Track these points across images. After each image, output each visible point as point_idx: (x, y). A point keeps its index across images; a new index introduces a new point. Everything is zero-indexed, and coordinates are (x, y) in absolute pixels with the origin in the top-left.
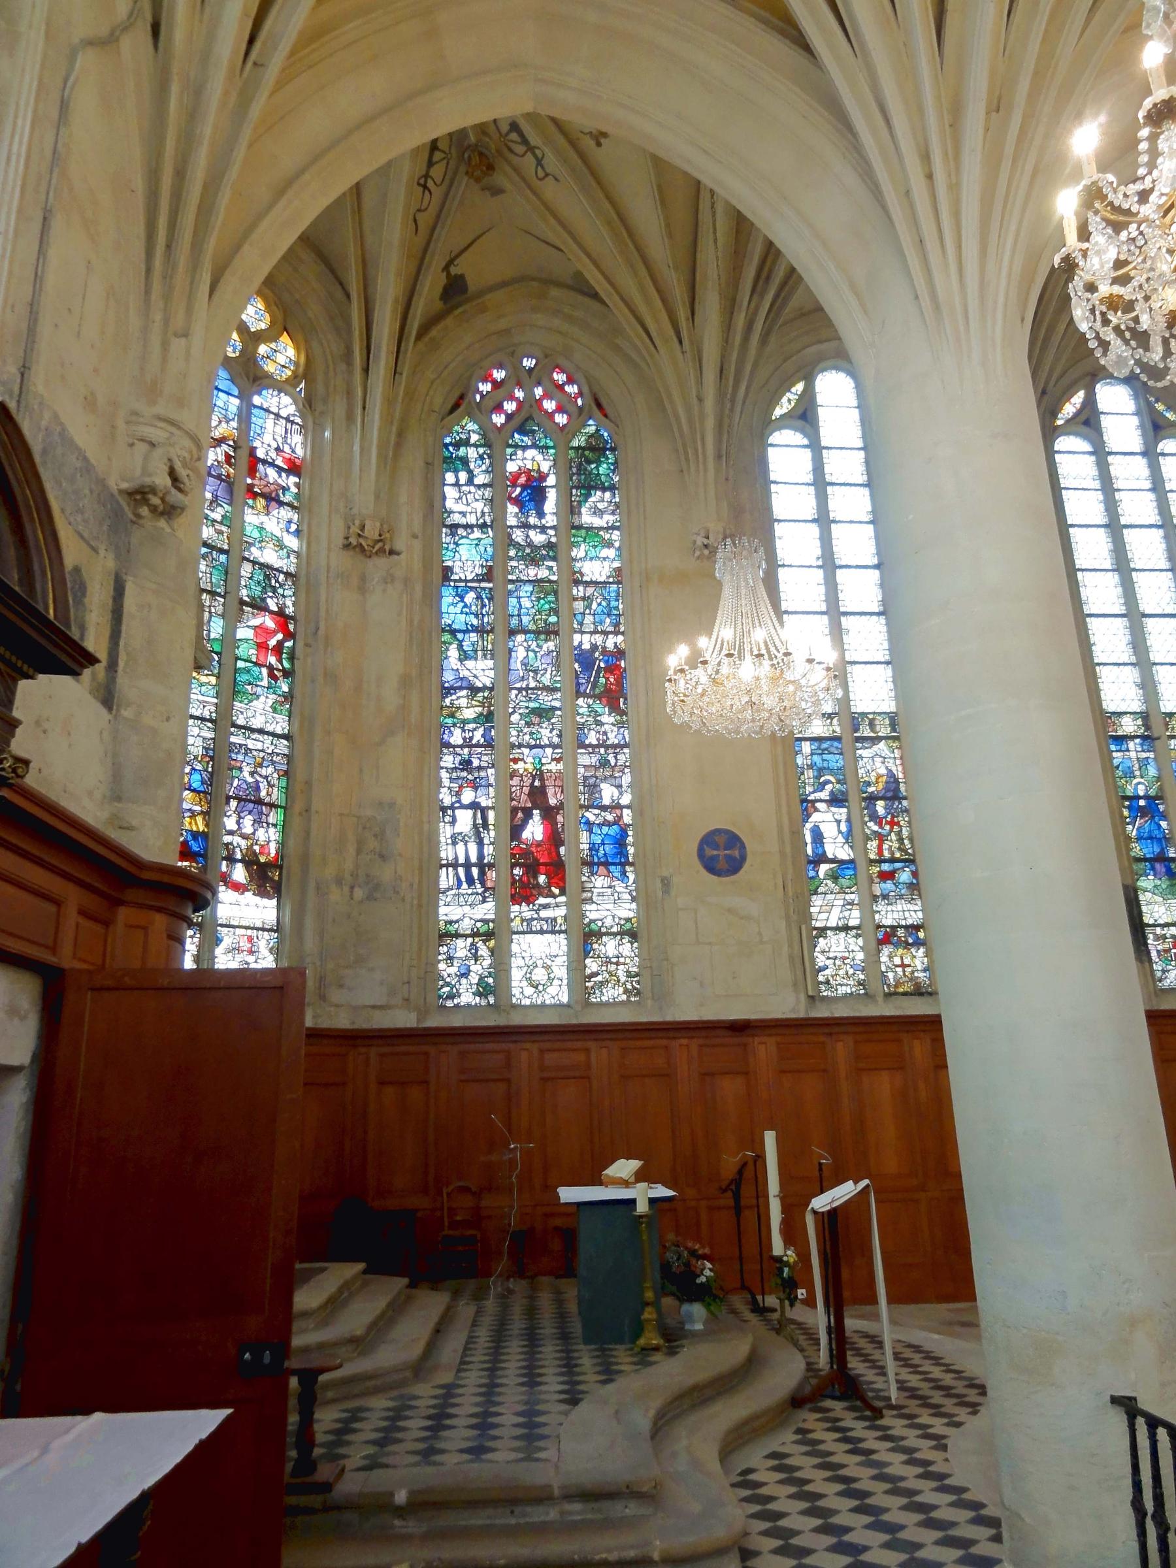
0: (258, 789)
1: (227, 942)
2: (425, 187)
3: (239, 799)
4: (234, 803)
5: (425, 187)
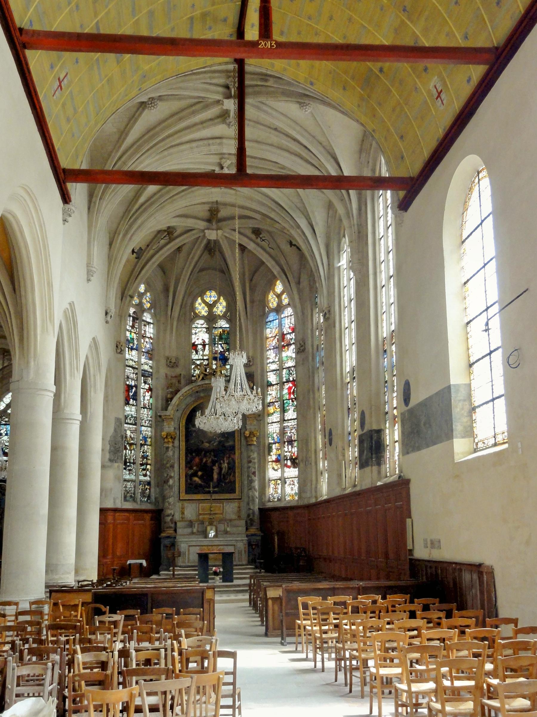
0: (291, 437)
1: (288, 483)
2: (263, 240)
3: (288, 442)
4: (286, 443)
5: (263, 240)
